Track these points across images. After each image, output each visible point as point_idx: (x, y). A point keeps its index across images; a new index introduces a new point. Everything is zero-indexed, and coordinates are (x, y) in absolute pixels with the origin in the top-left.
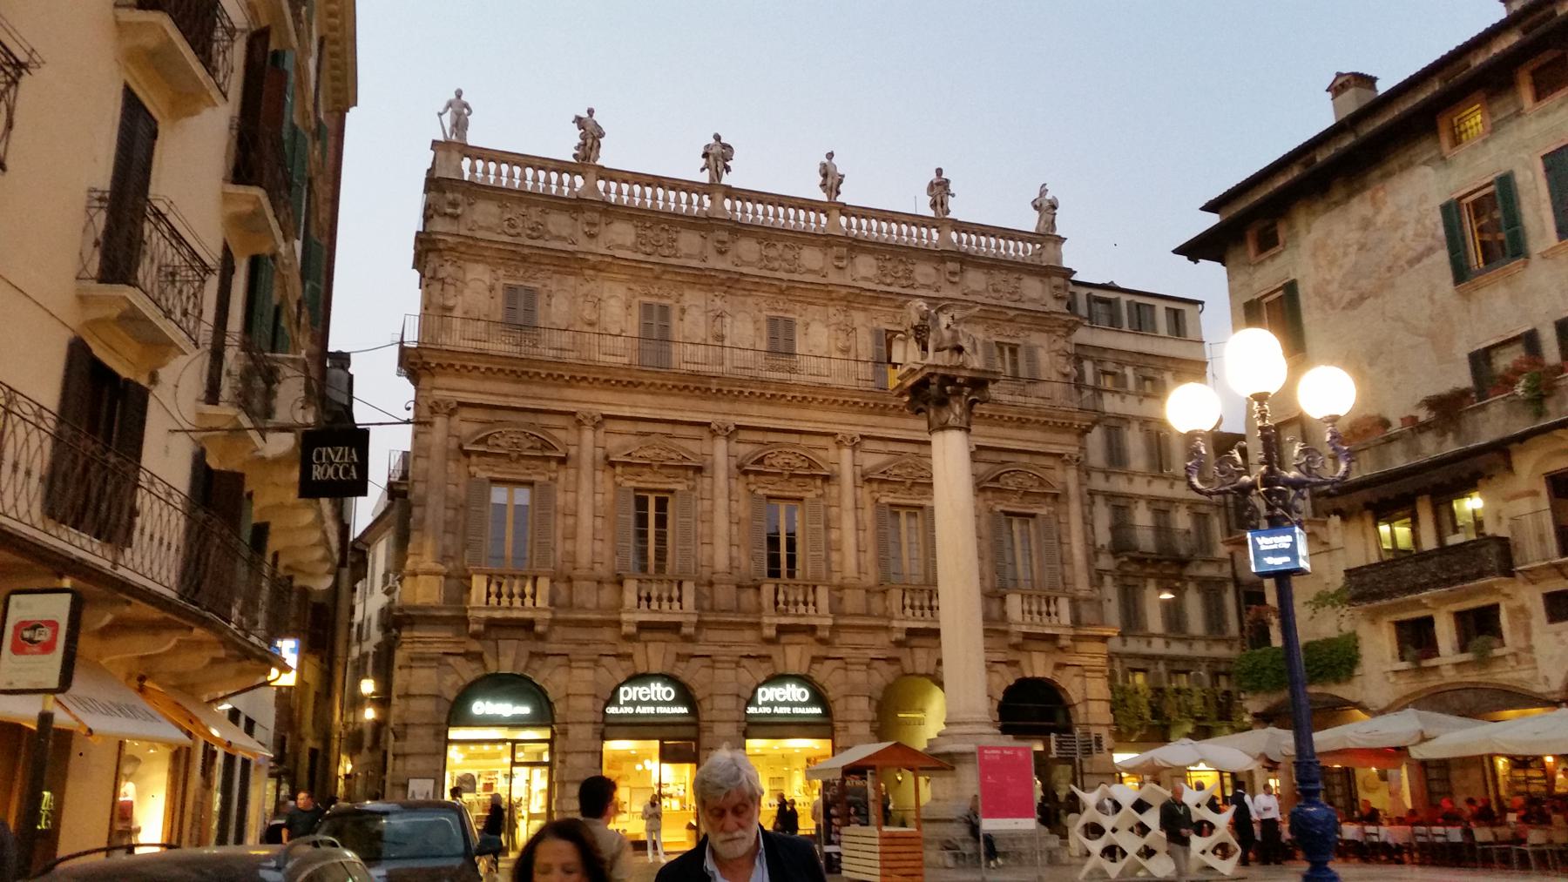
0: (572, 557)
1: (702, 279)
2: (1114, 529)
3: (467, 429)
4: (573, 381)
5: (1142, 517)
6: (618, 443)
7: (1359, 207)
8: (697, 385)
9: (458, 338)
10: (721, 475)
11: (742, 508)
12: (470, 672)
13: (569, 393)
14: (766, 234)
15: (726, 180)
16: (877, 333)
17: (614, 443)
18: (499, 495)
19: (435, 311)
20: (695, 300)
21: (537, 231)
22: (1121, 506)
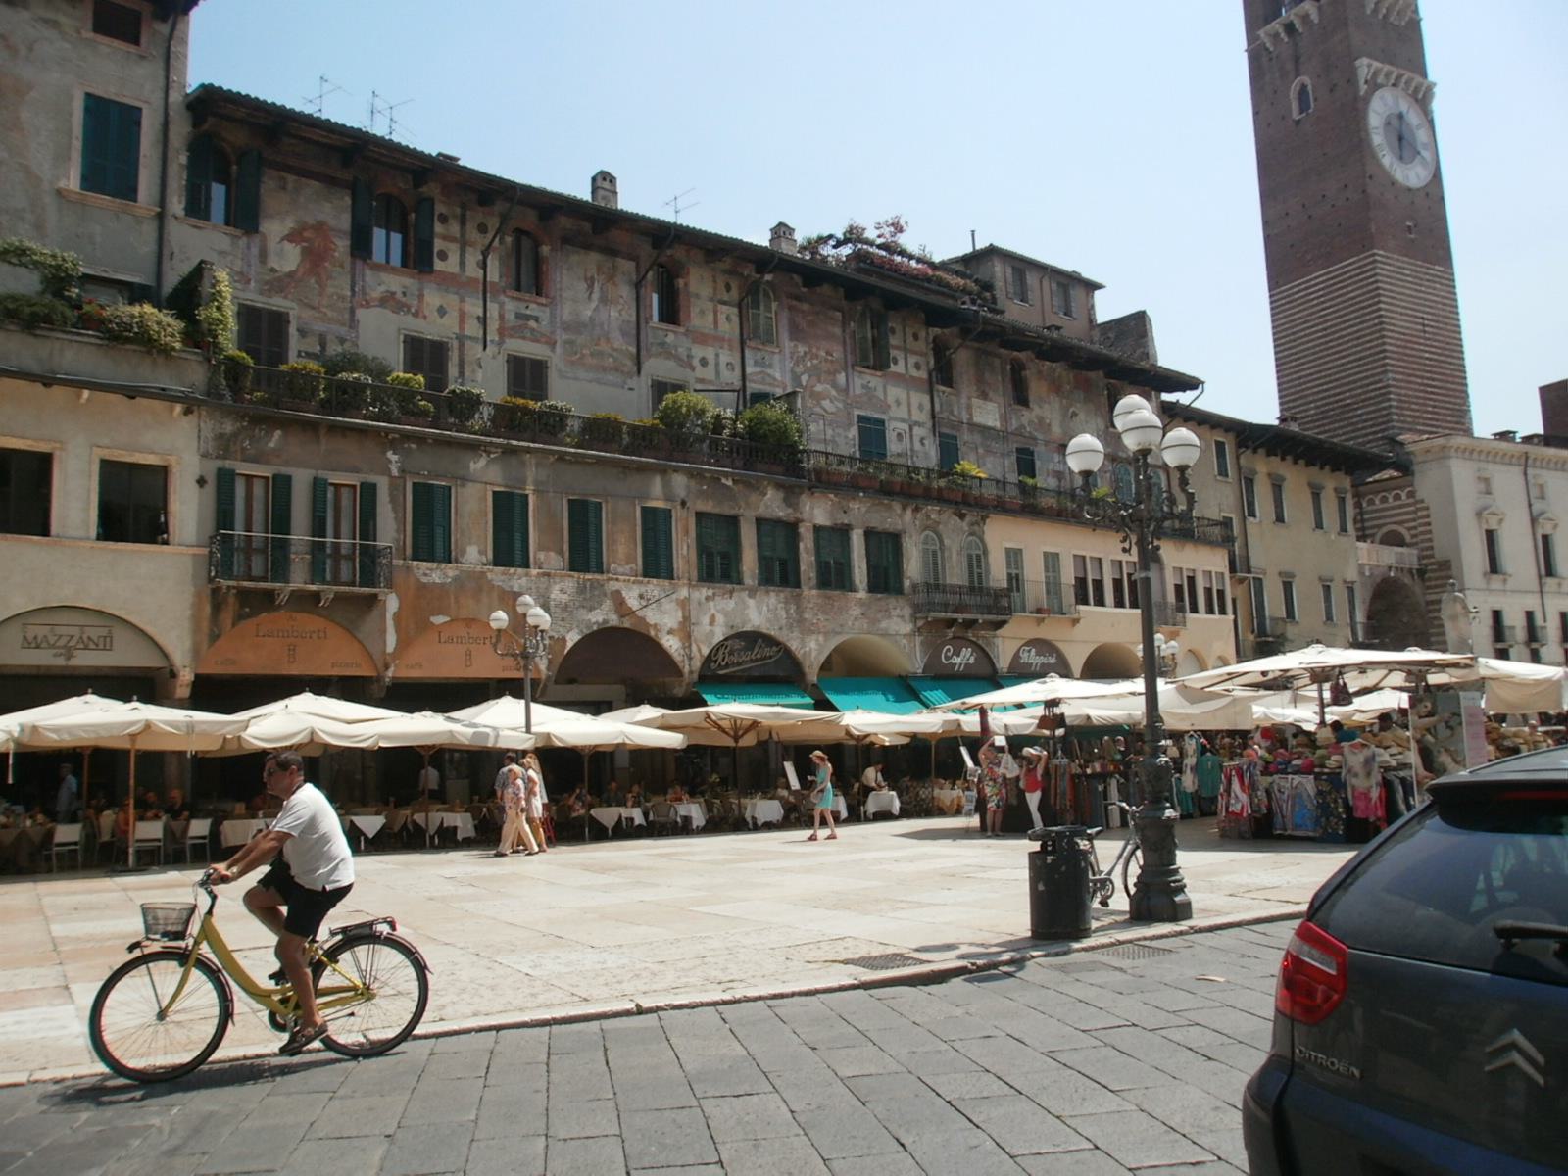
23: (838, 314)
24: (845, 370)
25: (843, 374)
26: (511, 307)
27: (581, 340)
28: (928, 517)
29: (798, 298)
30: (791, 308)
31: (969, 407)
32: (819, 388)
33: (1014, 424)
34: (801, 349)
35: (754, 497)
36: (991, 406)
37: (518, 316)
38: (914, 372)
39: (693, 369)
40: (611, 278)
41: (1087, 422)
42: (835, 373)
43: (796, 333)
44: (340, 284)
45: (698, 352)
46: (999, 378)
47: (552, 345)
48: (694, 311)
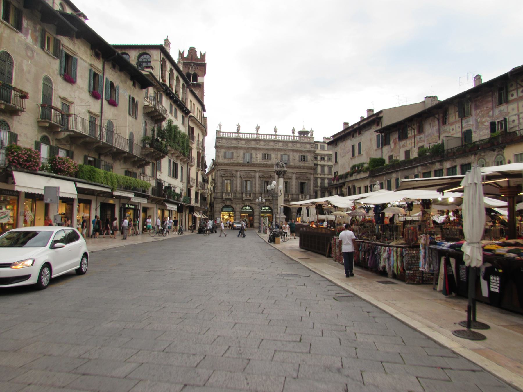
0: (236, 190)
1: (255, 149)
2: (321, 183)
3: (222, 173)
4: (236, 166)
5: (326, 181)
6: (243, 174)
7: (344, 143)
8: (254, 165)
9: (221, 160)
10: (257, 178)
11: (260, 182)
12: (224, 205)
14: (265, 141)
15: (259, 132)
16: (282, 156)
17: (242, 174)
18: (226, 181)
19: (217, 156)
20: (254, 152)
21: (231, 143)
22: (323, 179)
23: (491, 93)
24: (492, 109)
25: (492, 112)
26: (418, 137)
28: (481, 155)
29: (477, 97)
32: (484, 120)
34: (478, 111)
35: (433, 166)
37: (420, 138)
39: (450, 132)
40: (434, 121)
43: (477, 108)
44: (398, 147)
45: (451, 128)
47: (424, 141)
48: (451, 118)
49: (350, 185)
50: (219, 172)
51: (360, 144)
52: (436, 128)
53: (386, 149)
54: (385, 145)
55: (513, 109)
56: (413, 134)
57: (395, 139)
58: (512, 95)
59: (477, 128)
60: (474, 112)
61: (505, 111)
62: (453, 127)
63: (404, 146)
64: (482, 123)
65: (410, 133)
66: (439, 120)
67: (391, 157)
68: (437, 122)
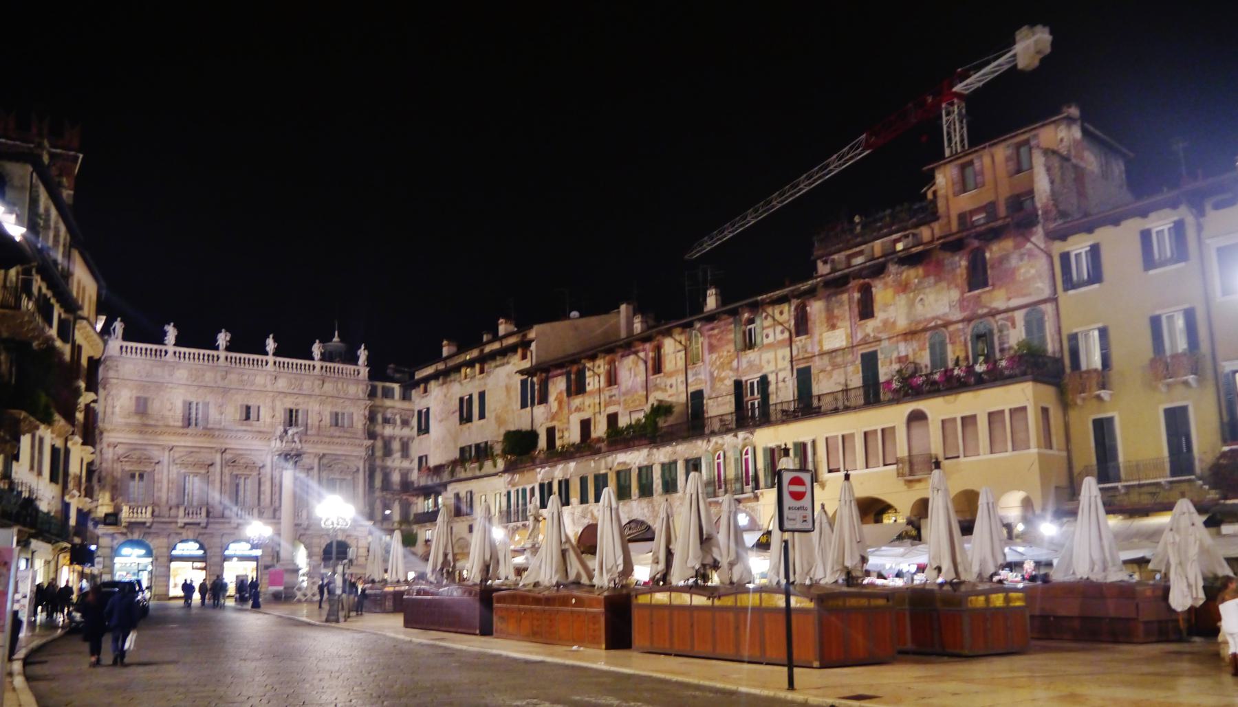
13: (160, 438)
26: (607, 393)
27: (628, 397)
29: (712, 329)
30: (710, 336)
31: (820, 342)
33: (860, 336)
34: (714, 356)
36: (838, 332)
38: (780, 337)
40: (637, 364)
41: (937, 301)
42: (731, 362)
43: (712, 349)
44: (566, 411)
45: (669, 382)
46: (847, 307)
49: (463, 494)
50: (111, 449)
51: (482, 395)
52: (641, 377)
53: (539, 410)
54: (540, 403)
55: (768, 362)
56: (597, 386)
57: (561, 393)
58: (767, 336)
59: (712, 388)
60: (707, 357)
61: (757, 362)
62: (673, 380)
63: (578, 409)
64: (722, 380)
65: (592, 383)
66: (646, 363)
67: (551, 432)
68: (642, 367)
